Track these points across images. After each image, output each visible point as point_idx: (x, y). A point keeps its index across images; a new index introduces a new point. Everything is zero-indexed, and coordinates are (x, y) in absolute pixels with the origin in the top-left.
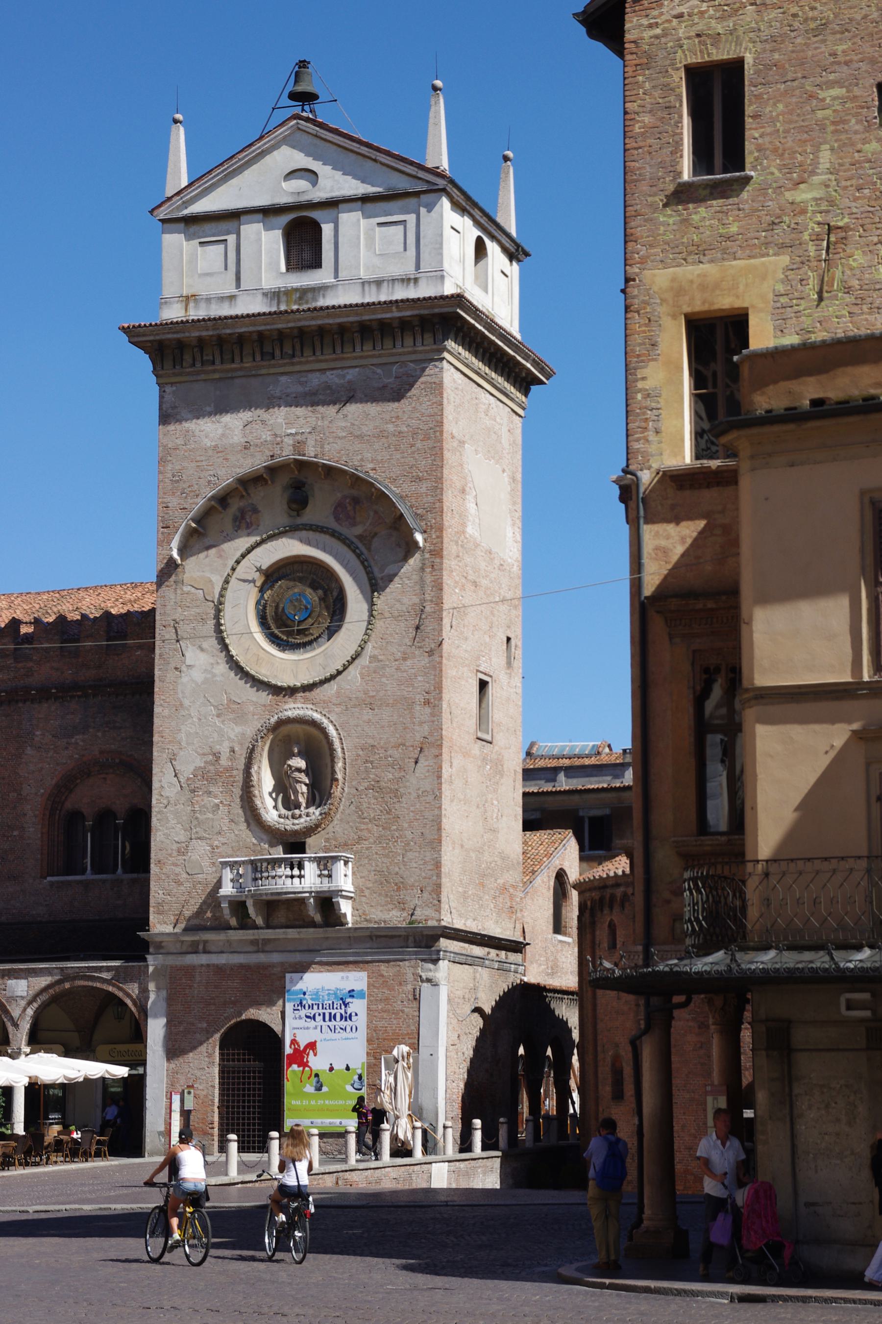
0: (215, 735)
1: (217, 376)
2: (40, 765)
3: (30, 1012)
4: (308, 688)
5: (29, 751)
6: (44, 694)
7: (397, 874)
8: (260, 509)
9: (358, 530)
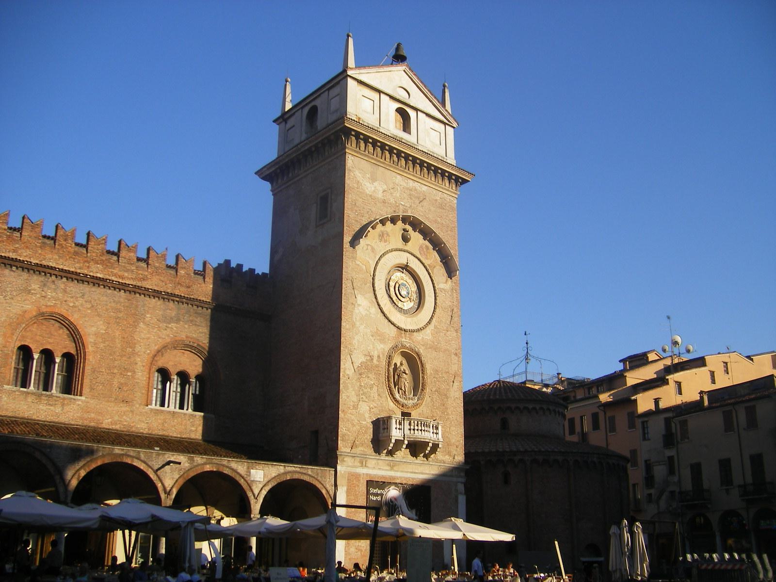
0: (371, 346)
1: (373, 161)
2: (148, 335)
3: (264, 492)
4: (413, 331)
5: (141, 325)
6: (156, 294)
7: (447, 437)
8: (390, 235)
9: (429, 263)
